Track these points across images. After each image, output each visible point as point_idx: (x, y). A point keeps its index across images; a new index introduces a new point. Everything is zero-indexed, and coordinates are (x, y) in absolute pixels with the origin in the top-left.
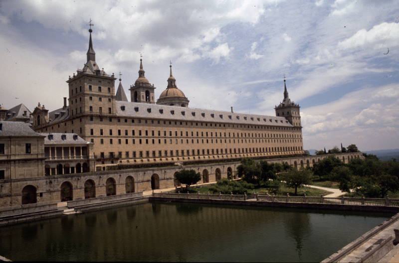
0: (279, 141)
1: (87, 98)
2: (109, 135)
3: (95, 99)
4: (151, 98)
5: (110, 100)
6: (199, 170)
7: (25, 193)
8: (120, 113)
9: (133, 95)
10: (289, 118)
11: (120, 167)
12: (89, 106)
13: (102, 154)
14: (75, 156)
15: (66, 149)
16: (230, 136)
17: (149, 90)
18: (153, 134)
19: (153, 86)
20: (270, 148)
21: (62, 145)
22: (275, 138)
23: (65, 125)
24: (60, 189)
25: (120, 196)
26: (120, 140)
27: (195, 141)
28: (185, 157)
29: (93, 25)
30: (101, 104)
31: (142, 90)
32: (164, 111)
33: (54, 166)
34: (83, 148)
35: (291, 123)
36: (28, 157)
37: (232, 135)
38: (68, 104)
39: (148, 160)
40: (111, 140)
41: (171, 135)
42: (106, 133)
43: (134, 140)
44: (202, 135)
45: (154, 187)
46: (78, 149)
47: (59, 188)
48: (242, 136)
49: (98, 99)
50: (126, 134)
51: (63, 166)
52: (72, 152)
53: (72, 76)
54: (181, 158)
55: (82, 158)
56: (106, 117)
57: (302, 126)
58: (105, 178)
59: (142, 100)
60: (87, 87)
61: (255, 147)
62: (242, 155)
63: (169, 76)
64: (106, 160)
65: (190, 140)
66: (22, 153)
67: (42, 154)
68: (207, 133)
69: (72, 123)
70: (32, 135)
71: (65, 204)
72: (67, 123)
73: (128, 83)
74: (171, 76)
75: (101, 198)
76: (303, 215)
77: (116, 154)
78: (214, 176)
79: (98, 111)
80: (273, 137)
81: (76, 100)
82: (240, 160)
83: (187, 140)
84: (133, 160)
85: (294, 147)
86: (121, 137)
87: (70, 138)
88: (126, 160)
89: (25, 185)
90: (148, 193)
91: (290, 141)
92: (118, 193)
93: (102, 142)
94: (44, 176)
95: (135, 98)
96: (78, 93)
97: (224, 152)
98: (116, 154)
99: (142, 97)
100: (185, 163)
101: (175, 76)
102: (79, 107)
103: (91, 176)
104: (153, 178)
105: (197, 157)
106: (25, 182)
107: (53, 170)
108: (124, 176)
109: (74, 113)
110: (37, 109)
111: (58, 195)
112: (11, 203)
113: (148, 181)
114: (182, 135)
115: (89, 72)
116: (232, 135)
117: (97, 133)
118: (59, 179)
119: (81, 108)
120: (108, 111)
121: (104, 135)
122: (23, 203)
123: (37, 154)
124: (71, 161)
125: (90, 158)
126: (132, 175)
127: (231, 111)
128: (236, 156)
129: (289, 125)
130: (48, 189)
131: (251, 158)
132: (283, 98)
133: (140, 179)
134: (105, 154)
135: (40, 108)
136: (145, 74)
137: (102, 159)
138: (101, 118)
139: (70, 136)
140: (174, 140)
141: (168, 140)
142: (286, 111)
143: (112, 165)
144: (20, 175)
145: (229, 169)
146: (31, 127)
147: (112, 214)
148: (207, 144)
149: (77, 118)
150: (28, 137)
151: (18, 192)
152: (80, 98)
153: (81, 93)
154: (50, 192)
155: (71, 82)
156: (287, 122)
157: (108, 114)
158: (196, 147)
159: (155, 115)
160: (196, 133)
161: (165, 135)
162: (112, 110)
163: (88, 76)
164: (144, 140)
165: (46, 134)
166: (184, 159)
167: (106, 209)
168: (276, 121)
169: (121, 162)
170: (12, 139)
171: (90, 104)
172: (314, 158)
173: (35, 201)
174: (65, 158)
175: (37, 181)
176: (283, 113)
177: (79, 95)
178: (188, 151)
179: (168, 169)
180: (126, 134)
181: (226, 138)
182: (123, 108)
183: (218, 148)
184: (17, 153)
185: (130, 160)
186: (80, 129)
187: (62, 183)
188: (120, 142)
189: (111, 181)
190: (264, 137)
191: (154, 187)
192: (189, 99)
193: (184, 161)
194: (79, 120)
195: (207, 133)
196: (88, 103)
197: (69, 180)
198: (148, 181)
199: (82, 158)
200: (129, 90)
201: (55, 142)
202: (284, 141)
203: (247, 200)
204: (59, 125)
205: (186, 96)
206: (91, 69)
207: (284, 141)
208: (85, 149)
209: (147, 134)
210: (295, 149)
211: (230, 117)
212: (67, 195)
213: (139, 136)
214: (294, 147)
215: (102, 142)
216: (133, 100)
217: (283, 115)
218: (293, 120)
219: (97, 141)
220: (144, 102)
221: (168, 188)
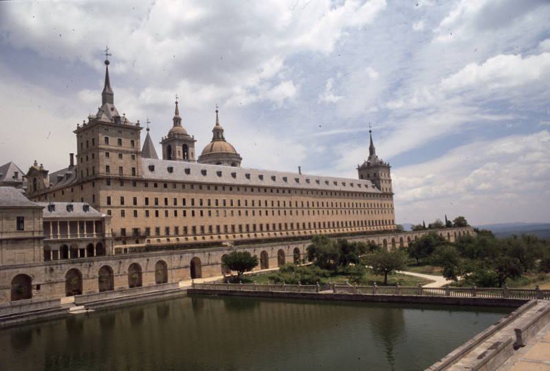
0: (363, 212)
1: (102, 154)
3: (114, 155)
5: (133, 157)
6: (255, 252)
7: (16, 285)
8: (148, 175)
9: (165, 150)
10: (376, 181)
11: (149, 249)
12: (105, 165)
13: (123, 231)
14: (85, 233)
16: (297, 205)
17: (187, 144)
18: (193, 204)
19: (193, 138)
21: (66, 218)
22: (356, 208)
24: (65, 279)
25: (148, 288)
26: (147, 212)
29: (110, 55)
30: (121, 162)
31: (177, 143)
33: (57, 247)
34: (96, 222)
37: (299, 205)
38: (75, 163)
39: (187, 239)
40: (135, 212)
41: (217, 204)
42: (129, 202)
43: (166, 212)
45: (194, 275)
46: (90, 224)
48: (313, 206)
50: (157, 203)
51: (69, 248)
52: (82, 228)
53: (81, 125)
55: (95, 237)
56: (129, 180)
57: (394, 191)
58: (127, 264)
59: (177, 157)
60: (102, 139)
62: (313, 231)
63: (214, 125)
64: (128, 238)
65: (243, 212)
66: (12, 230)
67: (40, 231)
69: (82, 189)
71: (72, 299)
73: (158, 134)
74: (217, 124)
75: (121, 291)
76: (395, 311)
77: (143, 230)
78: (276, 260)
79: (118, 172)
82: (310, 237)
83: (240, 212)
84: (165, 239)
85: (383, 221)
86: (150, 207)
87: (78, 210)
88: (155, 239)
89: (16, 274)
90: (186, 284)
91: (377, 212)
92: (145, 284)
93: (123, 214)
94: (42, 261)
95: (169, 154)
97: (289, 228)
98: (143, 230)
99: (177, 153)
100: (237, 243)
101: (222, 125)
102: (91, 167)
103: (108, 262)
105: (253, 234)
106: (16, 270)
107: (55, 252)
108: (154, 261)
109: (85, 175)
110: (32, 169)
113: (186, 267)
114: (232, 205)
115: (104, 118)
116: (299, 205)
117: (115, 202)
118: (63, 266)
119: (93, 168)
120: (130, 172)
121: (125, 205)
122: (13, 299)
123: (33, 232)
124: (80, 241)
125: (107, 236)
126: (164, 259)
127: (298, 172)
128: (305, 232)
129: (375, 190)
130: (48, 279)
131: (326, 235)
132: (368, 155)
133: (175, 264)
134: (127, 231)
136: (182, 122)
138: (122, 181)
139: (78, 207)
140: (221, 211)
141: (213, 211)
142: (372, 172)
143: (137, 245)
144: (9, 260)
145: (296, 251)
146: (24, 194)
147: (136, 312)
149: (88, 181)
150: (21, 208)
151: (5, 284)
152: (93, 155)
154: (50, 283)
155: (80, 132)
156: (373, 187)
158: (251, 220)
159: (196, 177)
161: (209, 204)
162: (136, 172)
163: (103, 124)
164: (180, 212)
165: (46, 204)
166: (234, 236)
167: (157, 301)
168: (359, 185)
169: (149, 241)
171: (106, 162)
172: (410, 235)
173: (30, 296)
174: (71, 236)
175: (32, 269)
177: (91, 150)
178: (240, 227)
179: (213, 251)
180: (157, 203)
181: (292, 208)
182: (152, 168)
183: (281, 222)
184: (5, 230)
185: (161, 239)
186: (92, 197)
187: (67, 271)
188: (147, 214)
189: (136, 268)
190: (343, 207)
192: (241, 156)
193: (235, 239)
194: (91, 183)
196: (104, 161)
197: (77, 266)
198: (186, 267)
199: (95, 237)
201: (58, 214)
202: (370, 212)
203: (320, 292)
204: (63, 192)
205: (238, 152)
206: (108, 115)
207: (370, 212)
208: (100, 223)
209: (184, 204)
210: (383, 222)
211: (297, 180)
213: (173, 206)
214: (383, 221)
215: (123, 214)
216: (166, 156)
217: (368, 177)
218: (381, 184)
219: (116, 212)
220: (180, 160)
221: (213, 277)
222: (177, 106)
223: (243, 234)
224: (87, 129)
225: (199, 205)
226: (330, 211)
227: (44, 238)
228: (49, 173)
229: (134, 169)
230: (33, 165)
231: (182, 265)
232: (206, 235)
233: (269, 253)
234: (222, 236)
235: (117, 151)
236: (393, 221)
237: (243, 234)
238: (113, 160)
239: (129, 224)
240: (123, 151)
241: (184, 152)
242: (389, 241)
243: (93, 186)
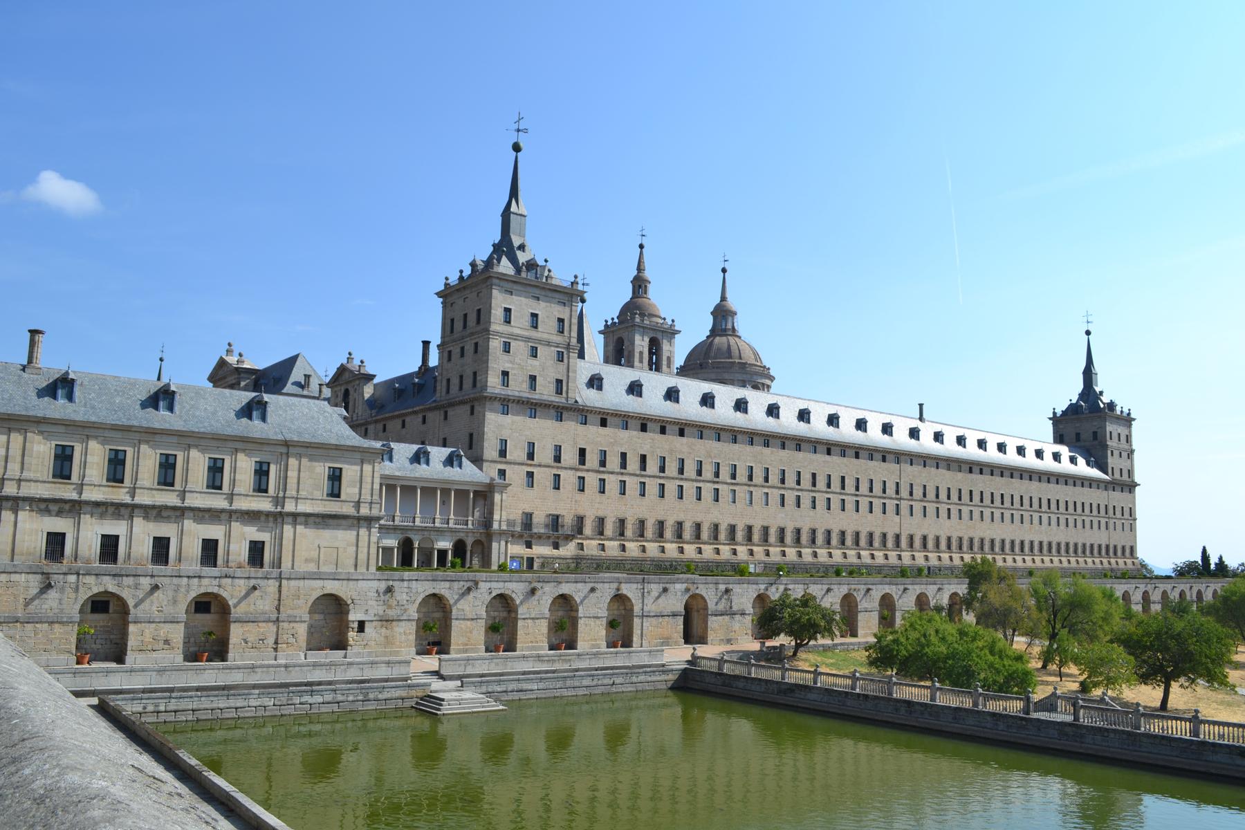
0: (1062, 521)
2: (550, 461)
4: (665, 362)
6: (830, 598)
7: (317, 617)
8: (589, 397)
9: (611, 348)
10: (1095, 451)
11: (579, 566)
13: (528, 517)
14: (452, 516)
15: (428, 492)
16: (911, 494)
17: (659, 336)
18: (681, 471)
20: (1032, 543)
21: (416, 479)
23: (424, 422)
24: (416, 616)
27: (806, 502)
28: (771, 549)
29: (526, 131)
31: (636, 333)
34: (475, 492)
35: (1103, 468)
36: (333, 507)
37: (918, 492)
38: (434, 361)
41: (734, 476)
42: (544, 454)
44: (829, 486)
46: (462, 494)
47: (413, 612)
48: (949, 498)
49: (527, 351)
53: (454, 279)
57: (1137, 480)
58: (548, 593)
59: (637, 363)
60: (497, 313)
62: (945, 556)
64: (540, 537)
65: (790, 497)
66: (318, 494)
68: (843, 478)
69: (446, 418)
70: (349, 443)
71: (431, 662)
72: (430, 415)
73: (601, 309)
74: (723, 298)
77: (568, 520)
78: (875, 617)
80: (1045, 507)
81: (462, 348)
82: (951, 572)
83: (783, 496)
84: (616, 543)
85: (1107, 546)
86: (588, 471)
87: (436, 466)
88: (595, 543)
90: (678, 655)
91: (1095, 525)
92: (582, 645)
94: (373, 569)
95: (618, 353)
96: (468, 331)
97: (890, 544)
98: (568, 520)
99: (637, 355)
100: (793, 569)
101: (733, 302)
104: (687, 607)
106: (319, 583)
107: (387, 551)
108: (606, 591)
110: (342, 370)
111: (406, 633)
112: (276, 643)
113: (674, 615)
115: (505, 267)
116: (918, 492)
117: (517, 452)
119: (475, 374)
120: (553, 387)
121: (536, 461)
125: (495, 526)
126: (630, 590)
128: (927, 558)
130: (381, 613)
131: (1015, 569)
133: (650, 607)
134: (535, 520)
135: (349, 366)
137: (526, 532)
138: (533, 408)
139: (438, 453)
140: (742, 492)
143: (555, 552)
144: (307, 561)
145: (921, 601)
146: (345, 418)
149: (462, 403)
150: (338, 448)
151: (296, 612)
152: (476, 344)
153: (479, 328)
154: (386, 621)
155: (447, 294)
157: (553, 399)
158: (806, 519)
159: (689, 408)
160: (809, 477)
161: (717, 475)
162: (564, 388)
163: (503, 278)
164: (652, 487)
165: (378, 445)
166: (768, 554)
168: (1056, 457)
169: (581, 546)
170: (292, 450)
172: (1168, 586)
173: (341, 645)
176: (1078, 435)
177: (472, 334)
182: (595, 382)
183: (873, 529)
186: (467, 439)
189: (564, 601)
191: (690, 636)
192: (772, 373)
194: (467, 407)
195: (843, 478)
196: (497, 361)
198: (674, 615)
199: (470, 526)
200: (600, 332)
202: (1079, 524)
203: (1035, 715)
204: (404, 422)
205: (766, 363)
207: (1079, 524)
208: (484, 495)
209: (662, 469)
210: (1109, 550)
212: (434, 639)
213: (638, 472)
214: (1107, 546)
218: (1110, 460)
219: (516, 475)
221: (731, 640)
222: (641, 253)
223: (786, 550)
224: (464, 288)
225: (693, 475)
226: (987, 513)
227: (379, 519)
228: (376, 381)
229: (559, 382)
230: (345, 362)
231: (668, 611)
232: (704, 543)
234: (739, 548)
235: (528, 339)
236: (1132, 549)
237: (786, 550)
238: (517, 360)
239: (541, 503)
240: (540, 341)
241: (651, 353)
242: (1137, 597)
243: (472, 413)
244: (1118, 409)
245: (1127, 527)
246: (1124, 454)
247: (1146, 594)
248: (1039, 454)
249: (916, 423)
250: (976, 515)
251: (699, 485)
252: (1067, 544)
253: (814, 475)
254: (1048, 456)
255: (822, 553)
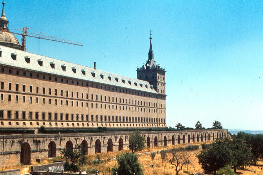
0: (143, 110)
10: (154, 83)
22: (137, 105)
27: (53, 102)
32: (17, 57)
54: (34, 123)
57: (166, 94)
61: (119, 115)
85: (157, 119)
113: (17, 153)
127: (94, 67)
129: (153, 91)
132: (147, 58)
140: (27, 97)
141: (20, 96)
148: (67, 107)
156: (151, 88)
161: (17, 89)
168: (141, 85)
178: (43, 114)
179: (163, 133)
183: (78, 113)
195: (67, 92)
198: (17, 153)
210: (157, 121)
217: (146, 79)
218: (158, 87)
225: (7, 89)
233: (89, 142)
234: (26, 122)
244: (161, 67)
245: (163, 112)
246: (163, 84)
247: (179, 136)
248: (136, 84)
249: (93, 70)
250: (115, 107)
251: (10, 94)
252: (144, 118)
253: (56, 90)
254: (138, 85)
255: (59, 124)
